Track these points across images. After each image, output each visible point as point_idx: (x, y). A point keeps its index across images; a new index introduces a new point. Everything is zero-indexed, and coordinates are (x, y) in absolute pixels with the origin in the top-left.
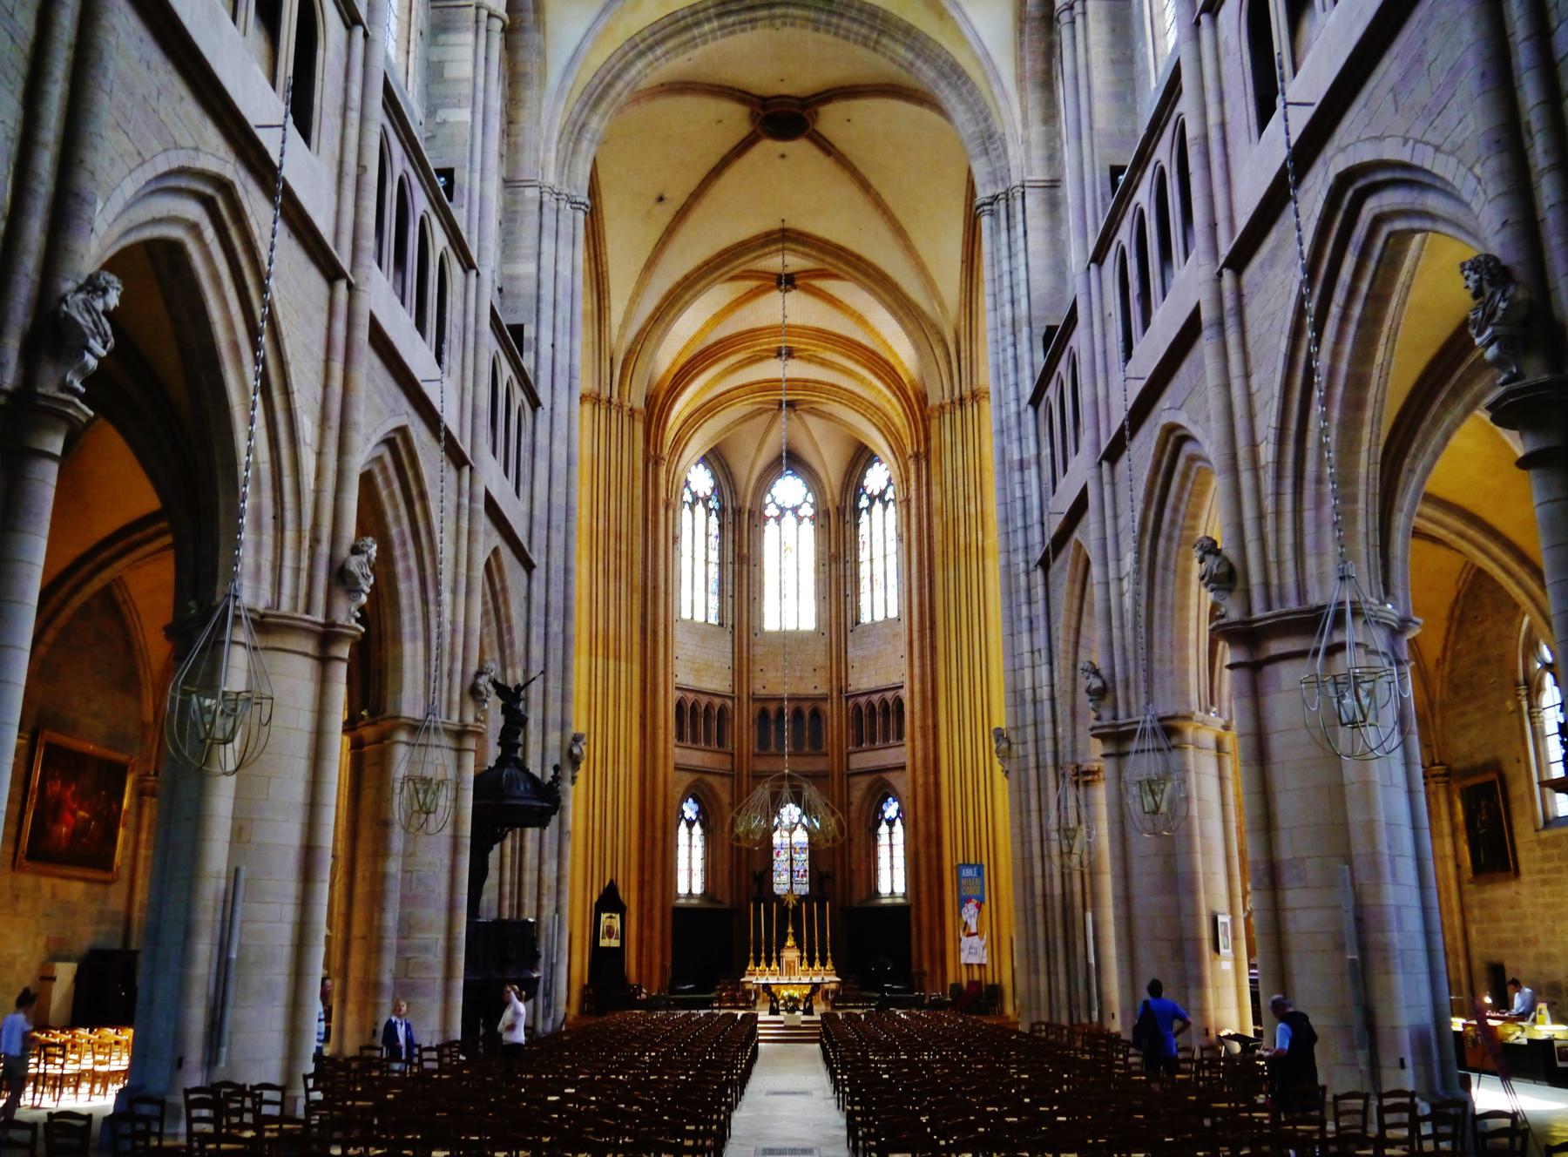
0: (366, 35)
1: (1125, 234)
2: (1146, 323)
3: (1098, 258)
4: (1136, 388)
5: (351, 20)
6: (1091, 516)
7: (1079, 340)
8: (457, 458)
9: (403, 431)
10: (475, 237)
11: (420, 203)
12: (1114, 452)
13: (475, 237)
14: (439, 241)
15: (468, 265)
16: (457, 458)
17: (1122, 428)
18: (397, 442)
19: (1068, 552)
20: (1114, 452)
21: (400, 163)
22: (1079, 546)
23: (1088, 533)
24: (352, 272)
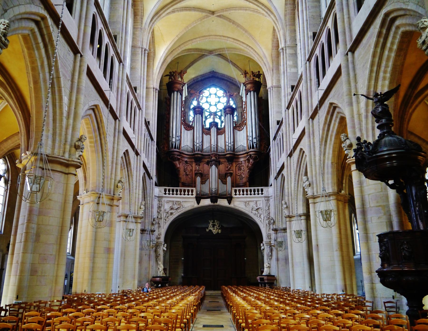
0: (123, 64)
1: (294, 103)
2: (298, 126)
3: (288, 108)
4: (294, 141)
5: (120, 61)
6: (285, 169)
7: (283, 127)
8: (137, 154)
9: (127, 151)
10: (141, 102)
11: (131, 97)
12: (290, 155)
13: (141, 102)
14: (135, 104)
15: (140, 109)
16: (137, 154)
17: (292, 150)
18: (126, 153)
19: (280, 176)
20: (290, 155)
21: (128, 89)
22: (283, 175)
23: (284, 172)
24: (119, 117)
